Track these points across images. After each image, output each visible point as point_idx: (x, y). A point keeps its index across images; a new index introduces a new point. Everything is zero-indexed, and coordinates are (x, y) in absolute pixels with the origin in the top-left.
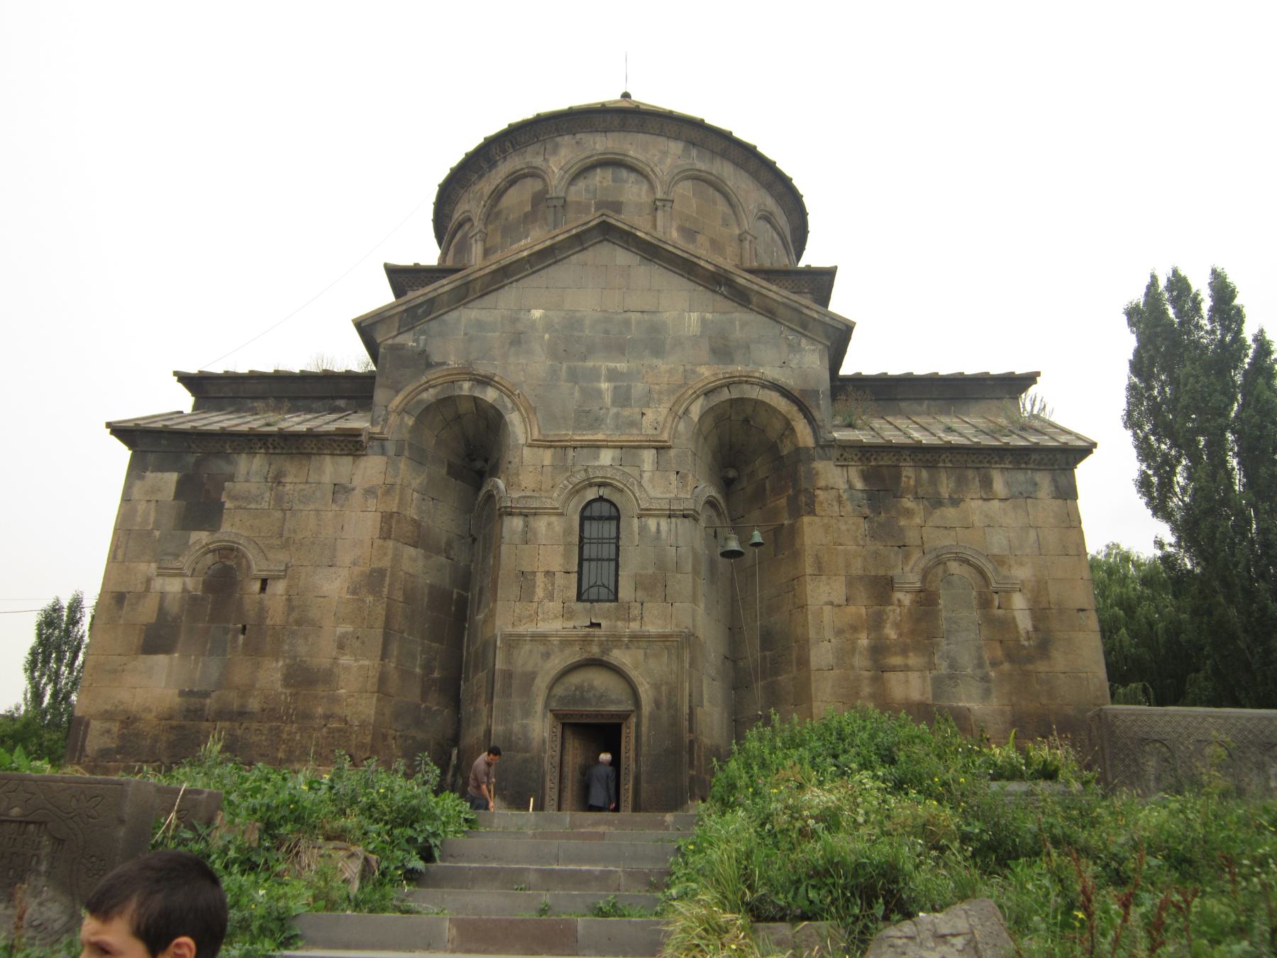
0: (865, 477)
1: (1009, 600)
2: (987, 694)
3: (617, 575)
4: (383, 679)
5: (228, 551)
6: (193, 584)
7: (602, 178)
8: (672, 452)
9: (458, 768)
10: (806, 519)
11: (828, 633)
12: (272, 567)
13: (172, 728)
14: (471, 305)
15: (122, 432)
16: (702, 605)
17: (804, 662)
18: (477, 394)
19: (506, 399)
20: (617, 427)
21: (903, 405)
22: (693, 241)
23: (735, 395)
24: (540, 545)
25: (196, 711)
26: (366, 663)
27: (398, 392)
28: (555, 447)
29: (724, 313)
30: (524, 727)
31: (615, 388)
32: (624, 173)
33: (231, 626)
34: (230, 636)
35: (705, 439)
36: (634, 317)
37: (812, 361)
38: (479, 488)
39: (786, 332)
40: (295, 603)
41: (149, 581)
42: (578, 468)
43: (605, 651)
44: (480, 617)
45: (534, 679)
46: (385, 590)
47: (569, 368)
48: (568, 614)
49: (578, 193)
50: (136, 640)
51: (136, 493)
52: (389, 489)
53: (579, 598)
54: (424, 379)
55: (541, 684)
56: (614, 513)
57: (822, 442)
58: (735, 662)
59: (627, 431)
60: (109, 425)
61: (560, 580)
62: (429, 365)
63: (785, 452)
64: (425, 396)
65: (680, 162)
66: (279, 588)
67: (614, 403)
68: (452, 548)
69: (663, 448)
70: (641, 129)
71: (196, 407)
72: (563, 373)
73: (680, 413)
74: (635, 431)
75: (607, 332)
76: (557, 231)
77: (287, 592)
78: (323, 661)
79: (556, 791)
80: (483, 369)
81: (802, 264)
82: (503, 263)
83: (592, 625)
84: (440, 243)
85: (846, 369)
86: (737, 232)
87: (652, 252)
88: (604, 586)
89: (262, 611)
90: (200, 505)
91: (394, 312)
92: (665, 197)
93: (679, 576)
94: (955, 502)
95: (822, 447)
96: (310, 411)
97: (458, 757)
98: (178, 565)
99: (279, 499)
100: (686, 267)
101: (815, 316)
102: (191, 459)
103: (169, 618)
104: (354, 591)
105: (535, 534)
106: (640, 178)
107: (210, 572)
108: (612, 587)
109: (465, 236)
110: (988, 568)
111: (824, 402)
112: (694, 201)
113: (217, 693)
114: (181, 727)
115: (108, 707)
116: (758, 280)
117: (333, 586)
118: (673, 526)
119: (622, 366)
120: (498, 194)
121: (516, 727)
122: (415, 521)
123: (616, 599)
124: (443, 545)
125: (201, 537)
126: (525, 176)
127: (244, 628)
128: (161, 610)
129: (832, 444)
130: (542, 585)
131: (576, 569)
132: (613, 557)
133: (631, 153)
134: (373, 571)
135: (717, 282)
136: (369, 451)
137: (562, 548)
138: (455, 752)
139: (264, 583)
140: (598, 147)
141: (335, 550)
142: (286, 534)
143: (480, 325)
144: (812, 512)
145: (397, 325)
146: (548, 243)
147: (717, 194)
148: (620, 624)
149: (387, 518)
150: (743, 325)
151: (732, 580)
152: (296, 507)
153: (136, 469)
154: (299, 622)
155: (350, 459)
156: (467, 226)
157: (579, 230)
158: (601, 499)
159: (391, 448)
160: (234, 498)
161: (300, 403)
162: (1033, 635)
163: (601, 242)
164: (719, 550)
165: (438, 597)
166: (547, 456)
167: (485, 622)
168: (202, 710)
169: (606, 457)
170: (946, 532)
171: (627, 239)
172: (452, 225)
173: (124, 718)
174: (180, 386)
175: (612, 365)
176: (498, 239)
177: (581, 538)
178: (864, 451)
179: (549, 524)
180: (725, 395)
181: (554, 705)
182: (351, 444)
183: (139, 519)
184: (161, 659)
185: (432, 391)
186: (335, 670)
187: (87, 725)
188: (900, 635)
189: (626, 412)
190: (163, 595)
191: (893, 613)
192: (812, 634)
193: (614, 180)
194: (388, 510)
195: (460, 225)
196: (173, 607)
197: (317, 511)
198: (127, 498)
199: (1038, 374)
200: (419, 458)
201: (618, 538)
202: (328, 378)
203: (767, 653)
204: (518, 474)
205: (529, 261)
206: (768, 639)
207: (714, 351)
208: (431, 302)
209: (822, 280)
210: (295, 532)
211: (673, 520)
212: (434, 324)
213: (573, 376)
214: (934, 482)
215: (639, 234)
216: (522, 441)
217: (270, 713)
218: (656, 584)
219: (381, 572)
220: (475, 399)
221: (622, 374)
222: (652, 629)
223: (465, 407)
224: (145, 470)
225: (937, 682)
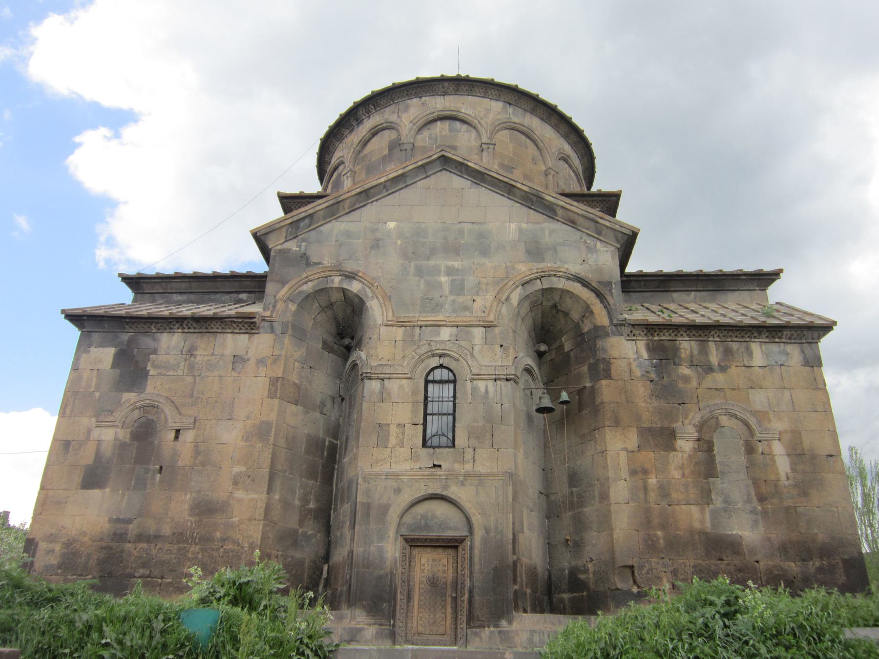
0: (649, 349)
1: (770, 446)
2: (755, 523)
3: (454, 426)
4: (268, 509)
5: (150, 408)
6: (124, 435)
7: (441, 128)
8: (497, 330)
9: (327, 580)
10: (604, 382)
11: (625, 473)
12: (184, 420)
13: (103, 548)
14: (341, 219)
16: (522, 451)
17: (604, 496)
18: (345, 286)
19: (367, 289)
20: (454, 311)
21: (675, 295)
22: (512, 173)
23: (546, 286)
24: (391, 403)
25: (121, 535)
26: (255, 496)
27: (283, 286)
28: (405, 326)
29: (537, 223)
30: (381, 550)
31: (452, 280)
32: (458, 124)
33: (151, 467)
34: (150, 475)
35: (523, 320)
36: (466, 227)
37: (605, 258)
38: (346, 359)
39: (585, 237)
40: (202, 448)
41: (89, 431)
42: (423, 342)
43: (446, 487)
44: (346, 460)
45: (387, 510)
46: (272, 439)
47: (416, 266)
48: (414, 457)
49: (424, 139)
50: (78, 478)
51: (82, 364)
52: (276, 359)
53: (424, 444)
54: (304, 275)
55: (393, 515)
56: (452, 377)
57: (615, 321)
58: (547, 496)
59: (461, 314)
60: (63, 311)
61: (409, 430)
62: (308, 264)
63: (586, 330)
64: (305, 287)
65: (499, 117)
66: (188, 436)
67: (451, 292)
68: (325, 405)
69: (489, 327)
70: (471, 92)
71: (135, 300)
72: (412, 270)
73: (503, 299)
74: (467, 314)
75: (445, 238)
76: (408, 163)
77: (195, 440)
78: (221, 495)
79: (405, 601)
80: (350, 266)
81: (594, 189)
82: (366, 187)
83: (435, 466)
84: (321, 183)
85: (631, 268)
86: (544, 168)
87: (479, 177)
88: (443, 435)
90: (131, 370)
91: (282, 224)
92: (488, 142)
93: (503, 427)
94: (723, 369)
95: (616, 325)
96: (222, 302)
97: (328, 573)
98: (112, 418)
99: (191, 367)
100: (508, 189)
101: (608, 224)
102: (125, 337)
103: (103, 460)
104: (247, 438)
105: (389, 394)
106: (470, 128)
107: (136, 424)
108: (450, 436)
109: (340, 175)
110: (752, 422)
111: (617, 290)
112: (511, 145)
113: (139, 520)
114: (110, 548)
115: (53, 531)
116: (563, 198)
117: (230, 436)
118: (498, 387)
119: (457, 264)
120: (365, 143)
121: (373, 549)
122: (294, 384)
123: (454, 446)
124: (318, 402)
125: (130, 397)
126: (384, 129)
127: (161, 467)
128: (98, 455)
129: (622, 324)
130: (395, 434)
131: (422, 422)
132: (451, 411)
133: (463, 111)
134: (262, 423)
135: (533, 201)
136: (261, 330)
137: (410, 406)
138: (326, 567)
139: (178, 431)
140: (438, 106)
141: (233, 407)
142: (195, 393)
143: (348, 234)
144: (609, 377)
145: (284, 234)
146: (400, 172)
147: (528, 140)
148: (457, 466)
149: (274, 381)
150: (551, 232)
151: (545, 431)
152: (203, 374)
153: (83, 346)
154: (203, 464)
155: (247, 336)
156: (341, 168)
157: (424, 162)
158: (441, 366)
159: (278, 327)
160: (155, 367)
161: (213, 296)
162: (791, 475)
163: (441, 170)
164: (535, 407)
165: (314, 444)
166: (399, 333)
167: (350, 463)
168: (126, 534)
169: (446, 334)
170: (717, 392)
171: (463, 169)
172: (330, 168)
173: (65, 540)
174: (124, 285)
175: (450, 263)
176: (363, 176)
177: (426, 397)
178: (650, 328)
179: (401, 386)
180: (538, 285)
181: (404, 531)
182: (247, 324)
183: (84, 384)
184: (96, 493)
185: (309, 283)
186: (231, 502)
187: (37, 544)
188: (683, 475)
189: (461, 299)
190: (99, 442)
192: (611, 474)
193: (450, 130)
194: (275, 375)
195: (336, 169)
196: (108, 450)
197: (220, 376)
198: (75, 368)
199: (781, 271)
200: (299, 334)
201: (454, 397)
202: (234, 277)
203: (574, 489)
204: (376, 348)
205: (385, 187)
206: (574, 478)
207: (529, 252)
208: (311, 216)
209: (609, 202)
210: (203, 393)
211: (498, 382)
212: (313, 233)
213: (419, 272)
214: (704, 351)
215: (470, 164)
216: (380, 322)
217: (180, 537)
218: (486, 434)
219: (269, 424)
220: (344, 290)
221: (457, 270)
222: (481, 469)
223: (336, 297)
224: (90, 346)
225: (715, 515)
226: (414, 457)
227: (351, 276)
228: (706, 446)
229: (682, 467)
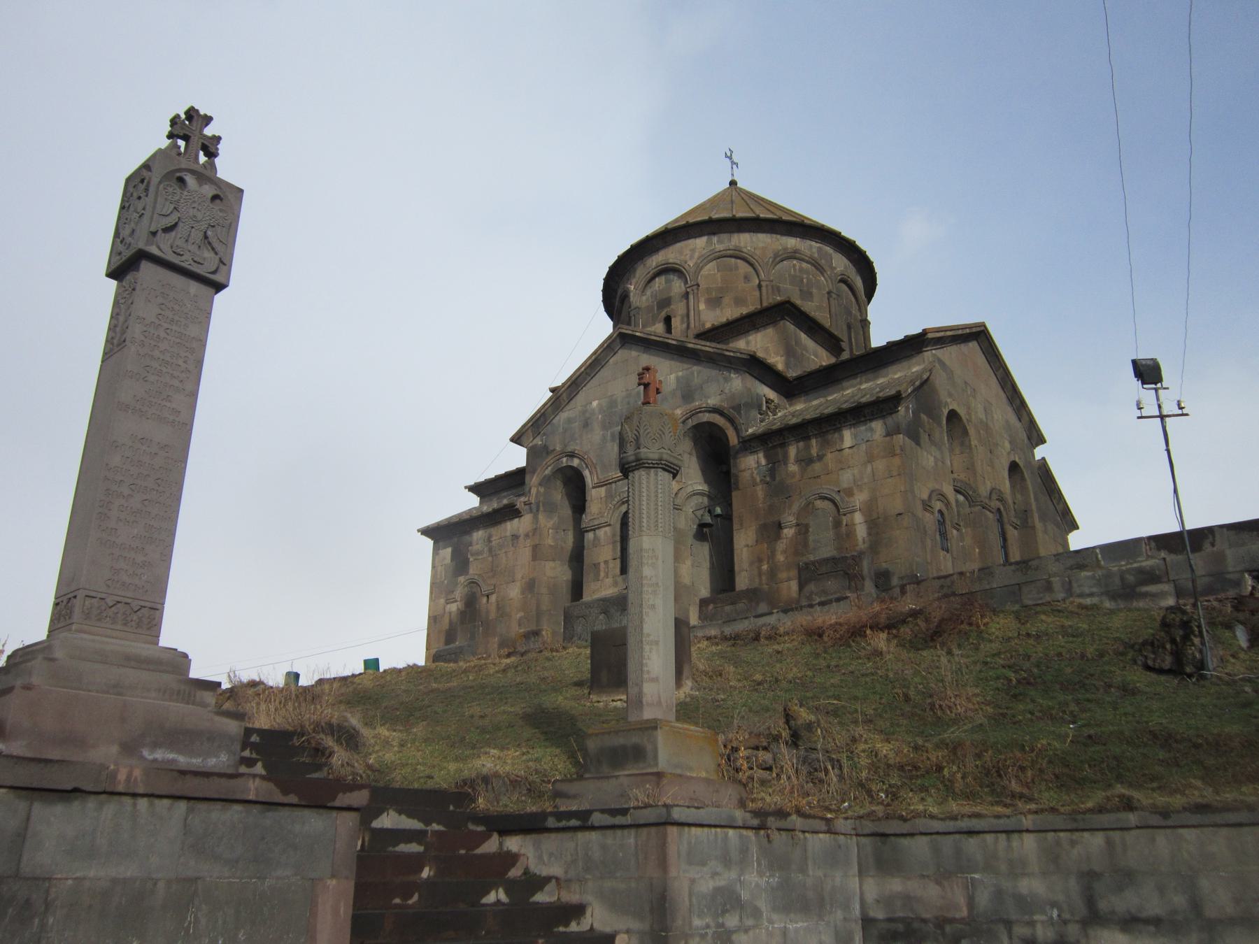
5: (473, 583)
7: (659, 282)
11: (746, 566)
15: (426, 532)
16: (689, 563)
48: (615, 584)
62: (548, 453)
66: (493, 598)
71: (481, 503)
72: (609, 438)
89: (488, 612)
90: (461, 563)
99: (490, 550)
104: (523, 593)
110: (837, 498)
125: (462, 579)
128: (451, 623)
131: (619, 554)
143: (569, 421)
144: (737, 488)
166: (603, 490)
191: (781, 546)
198: (433, 567)
214: (808, 447)
226: (615, 584)
227: (572, 455)
228: (803, 529)
229: (784, 552)
